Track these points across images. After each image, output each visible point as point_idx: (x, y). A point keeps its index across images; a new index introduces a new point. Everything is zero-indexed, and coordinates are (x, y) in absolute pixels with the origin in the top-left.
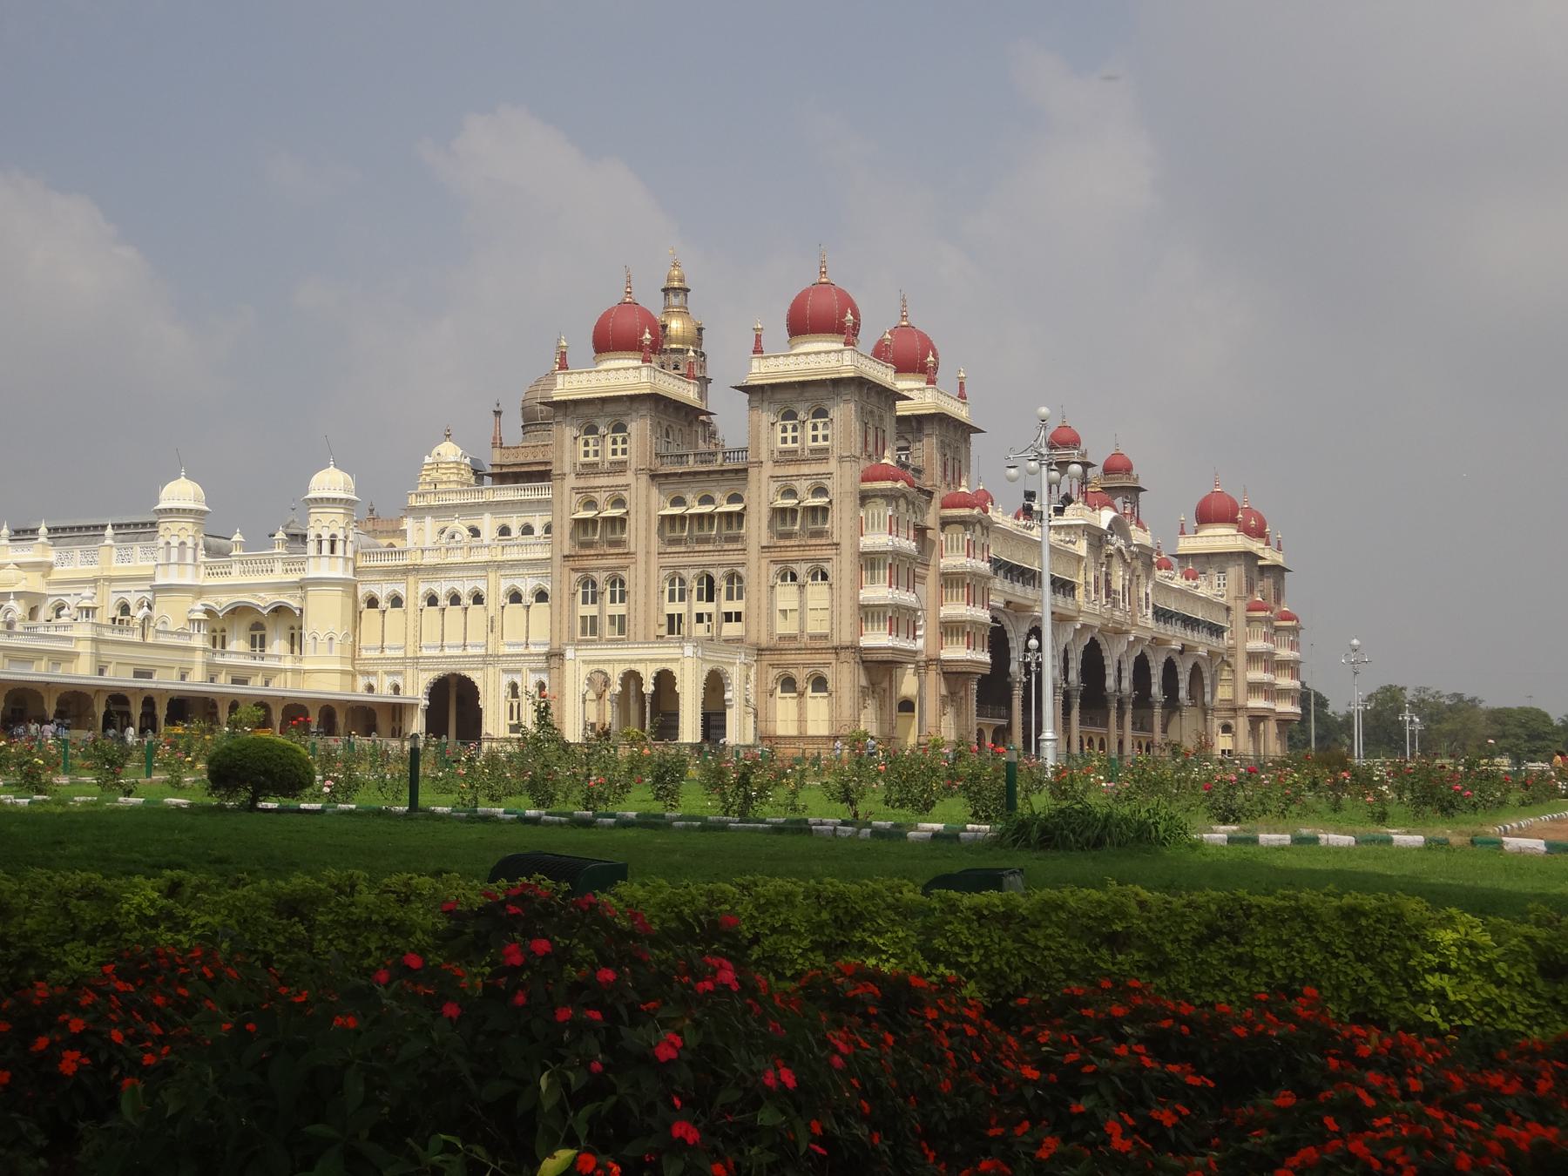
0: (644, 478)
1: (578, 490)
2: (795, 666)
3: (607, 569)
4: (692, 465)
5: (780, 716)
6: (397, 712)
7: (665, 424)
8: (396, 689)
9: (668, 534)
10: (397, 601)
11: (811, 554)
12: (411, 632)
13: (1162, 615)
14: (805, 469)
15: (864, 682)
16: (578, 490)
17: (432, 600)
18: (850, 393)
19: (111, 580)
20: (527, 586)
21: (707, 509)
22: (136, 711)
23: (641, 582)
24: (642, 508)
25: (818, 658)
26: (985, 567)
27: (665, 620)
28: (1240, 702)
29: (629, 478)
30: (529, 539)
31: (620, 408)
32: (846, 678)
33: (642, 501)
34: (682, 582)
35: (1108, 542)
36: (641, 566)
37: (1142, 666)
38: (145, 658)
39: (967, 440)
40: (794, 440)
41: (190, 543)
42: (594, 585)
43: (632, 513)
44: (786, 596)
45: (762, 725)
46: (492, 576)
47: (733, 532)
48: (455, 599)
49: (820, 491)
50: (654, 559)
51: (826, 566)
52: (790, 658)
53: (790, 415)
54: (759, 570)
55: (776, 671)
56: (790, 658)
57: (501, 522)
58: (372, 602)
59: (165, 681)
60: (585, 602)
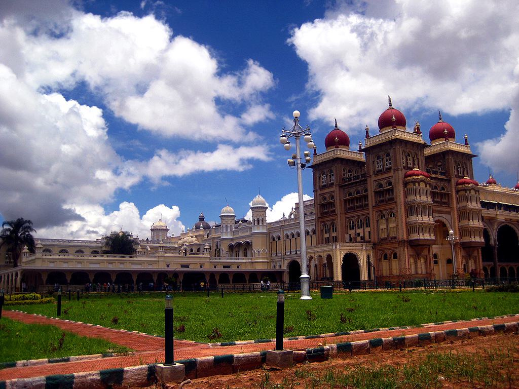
0: (337, 188)
3: (330, 220)
5: (384, 268)
7: (348, 169)
10: (279, 238)
14: (384, 176)
17: (288, 237)
24: (338, 198)
25: (393, 246)
26: (480, 206)
33: (338, 195)
36: (339, 219)
38: (185, 261)
45: (376, 273)
52: (385, 246)
54: (373, 215)
55: (380, 252)
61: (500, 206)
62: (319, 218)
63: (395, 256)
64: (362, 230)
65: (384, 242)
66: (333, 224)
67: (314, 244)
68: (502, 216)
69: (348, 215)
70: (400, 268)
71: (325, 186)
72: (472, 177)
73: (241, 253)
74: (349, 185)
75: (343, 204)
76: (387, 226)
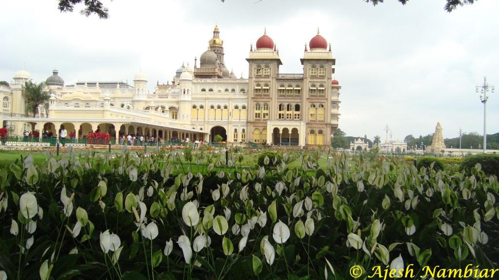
0: (274, 80)
1: (256, 82)
6: (202, 136)
8: (201, 129)
9: (279, 94)
14: (319, 80)
16: (256, 82)
17: (212, 107)
19: (119, 98)
20: (240, 105)
24: (274, 87)
25: (321, 126)
27: (278, 115)
30: (227, 92)
31: (268, 62)
33: (274, 85)
34: (283, 106)
40: (315, 73)
42: (259, 105)
43: (271, 88)
44: (312, 111)
47: (297, 94)
48: (219, 107)
49: (321, 86)
50: (276, 99)
51: (323, 104)
52: (314, 126)
53: (314, 67)
56: (314, 126)
57: (226, 88)
58: (194, 107)
60: (256, 109)
70: (324, 141)
71: (260, 75)
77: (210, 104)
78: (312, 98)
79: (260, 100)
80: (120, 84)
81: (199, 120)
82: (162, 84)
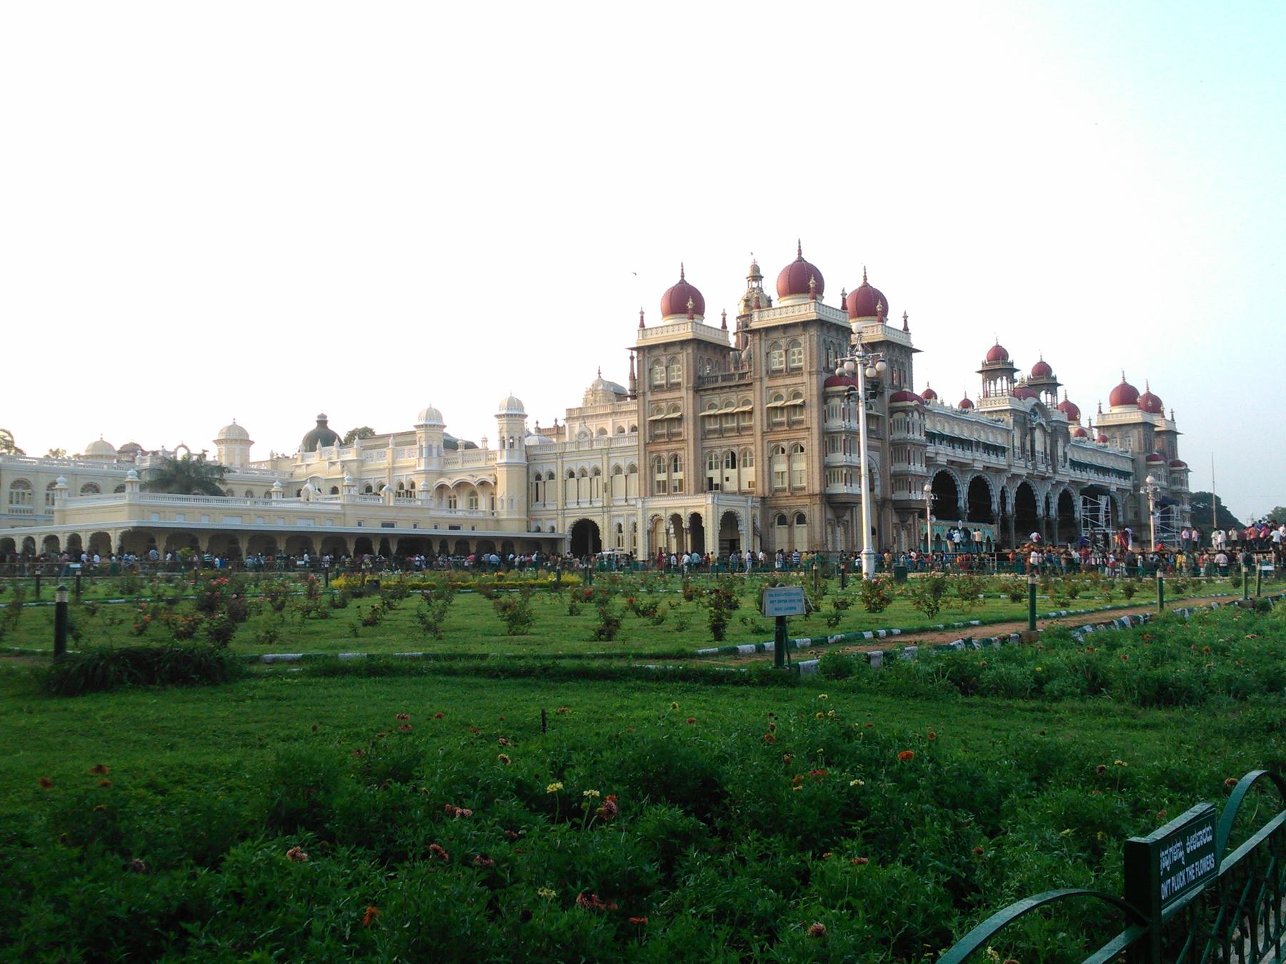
0: (691, 392)
2: (785, 507)
4: (720, 384)
6: (554, 543)
8: (553, 529)
10: (551, 476)
11: (792, 435)
12: (560, 494)
13: (1076, 465)
14: (789, 381)
15: (830, 515)
17: (572, 475)
18: (813, 332)
21: (729, 410)
22: (376, 548)
23: (692, 457)
24: (691, 411)
25: (799, 502)
27: (706, 481)
28: (1143, 521)
29: (683, 393)
31: (677, 349)
32: (815, 512)
33: (691, 406)
35: (1031, 421)
37: (1066, 500)
38: (389, 516)
39: (910, 358)
41: (435, 445)
46: (605, 458)
47: (746, 424)
51: (803, 443)
56: (783, 502)
59: (403, 528)
61: (942, 438)
62: (646, 444)
63: (801, 519)
64: (735, 471)
65: (780, 494)
66: (676, 458)
67: (634, 492)
68: (944, 453)
69: (708, 443)
70: (811, 540)
71: (661, 386)
72: (911, 387)
73: (462, 503)
74: (713, 389)
75: (699, 423)
76: (790, 468)
77: (566, 467)
78: (776, 429)
79: (664, 447)
80: (396, 435)
81: (548, 507)
82: (551, 425)
